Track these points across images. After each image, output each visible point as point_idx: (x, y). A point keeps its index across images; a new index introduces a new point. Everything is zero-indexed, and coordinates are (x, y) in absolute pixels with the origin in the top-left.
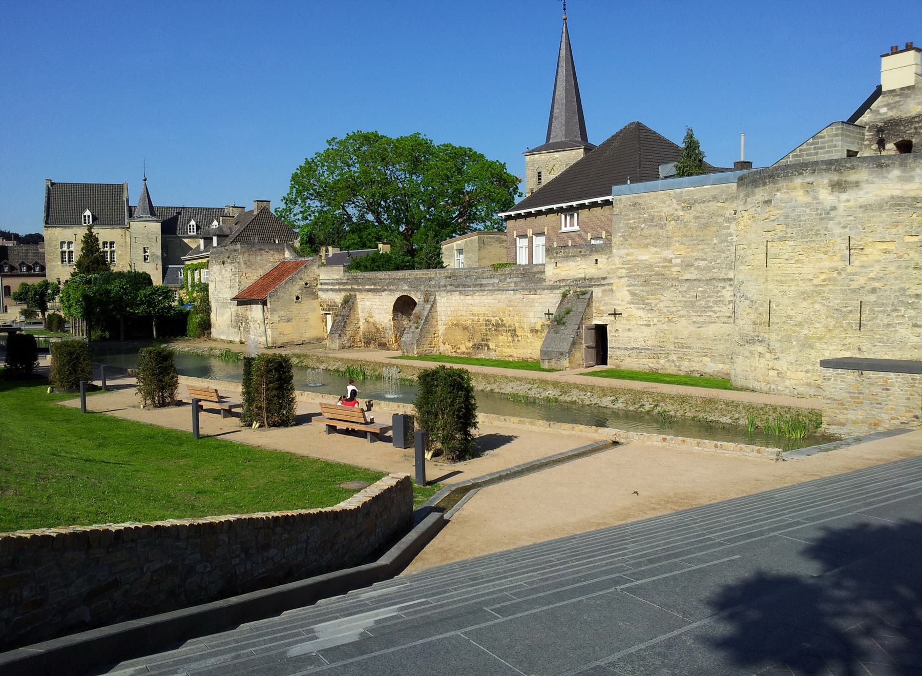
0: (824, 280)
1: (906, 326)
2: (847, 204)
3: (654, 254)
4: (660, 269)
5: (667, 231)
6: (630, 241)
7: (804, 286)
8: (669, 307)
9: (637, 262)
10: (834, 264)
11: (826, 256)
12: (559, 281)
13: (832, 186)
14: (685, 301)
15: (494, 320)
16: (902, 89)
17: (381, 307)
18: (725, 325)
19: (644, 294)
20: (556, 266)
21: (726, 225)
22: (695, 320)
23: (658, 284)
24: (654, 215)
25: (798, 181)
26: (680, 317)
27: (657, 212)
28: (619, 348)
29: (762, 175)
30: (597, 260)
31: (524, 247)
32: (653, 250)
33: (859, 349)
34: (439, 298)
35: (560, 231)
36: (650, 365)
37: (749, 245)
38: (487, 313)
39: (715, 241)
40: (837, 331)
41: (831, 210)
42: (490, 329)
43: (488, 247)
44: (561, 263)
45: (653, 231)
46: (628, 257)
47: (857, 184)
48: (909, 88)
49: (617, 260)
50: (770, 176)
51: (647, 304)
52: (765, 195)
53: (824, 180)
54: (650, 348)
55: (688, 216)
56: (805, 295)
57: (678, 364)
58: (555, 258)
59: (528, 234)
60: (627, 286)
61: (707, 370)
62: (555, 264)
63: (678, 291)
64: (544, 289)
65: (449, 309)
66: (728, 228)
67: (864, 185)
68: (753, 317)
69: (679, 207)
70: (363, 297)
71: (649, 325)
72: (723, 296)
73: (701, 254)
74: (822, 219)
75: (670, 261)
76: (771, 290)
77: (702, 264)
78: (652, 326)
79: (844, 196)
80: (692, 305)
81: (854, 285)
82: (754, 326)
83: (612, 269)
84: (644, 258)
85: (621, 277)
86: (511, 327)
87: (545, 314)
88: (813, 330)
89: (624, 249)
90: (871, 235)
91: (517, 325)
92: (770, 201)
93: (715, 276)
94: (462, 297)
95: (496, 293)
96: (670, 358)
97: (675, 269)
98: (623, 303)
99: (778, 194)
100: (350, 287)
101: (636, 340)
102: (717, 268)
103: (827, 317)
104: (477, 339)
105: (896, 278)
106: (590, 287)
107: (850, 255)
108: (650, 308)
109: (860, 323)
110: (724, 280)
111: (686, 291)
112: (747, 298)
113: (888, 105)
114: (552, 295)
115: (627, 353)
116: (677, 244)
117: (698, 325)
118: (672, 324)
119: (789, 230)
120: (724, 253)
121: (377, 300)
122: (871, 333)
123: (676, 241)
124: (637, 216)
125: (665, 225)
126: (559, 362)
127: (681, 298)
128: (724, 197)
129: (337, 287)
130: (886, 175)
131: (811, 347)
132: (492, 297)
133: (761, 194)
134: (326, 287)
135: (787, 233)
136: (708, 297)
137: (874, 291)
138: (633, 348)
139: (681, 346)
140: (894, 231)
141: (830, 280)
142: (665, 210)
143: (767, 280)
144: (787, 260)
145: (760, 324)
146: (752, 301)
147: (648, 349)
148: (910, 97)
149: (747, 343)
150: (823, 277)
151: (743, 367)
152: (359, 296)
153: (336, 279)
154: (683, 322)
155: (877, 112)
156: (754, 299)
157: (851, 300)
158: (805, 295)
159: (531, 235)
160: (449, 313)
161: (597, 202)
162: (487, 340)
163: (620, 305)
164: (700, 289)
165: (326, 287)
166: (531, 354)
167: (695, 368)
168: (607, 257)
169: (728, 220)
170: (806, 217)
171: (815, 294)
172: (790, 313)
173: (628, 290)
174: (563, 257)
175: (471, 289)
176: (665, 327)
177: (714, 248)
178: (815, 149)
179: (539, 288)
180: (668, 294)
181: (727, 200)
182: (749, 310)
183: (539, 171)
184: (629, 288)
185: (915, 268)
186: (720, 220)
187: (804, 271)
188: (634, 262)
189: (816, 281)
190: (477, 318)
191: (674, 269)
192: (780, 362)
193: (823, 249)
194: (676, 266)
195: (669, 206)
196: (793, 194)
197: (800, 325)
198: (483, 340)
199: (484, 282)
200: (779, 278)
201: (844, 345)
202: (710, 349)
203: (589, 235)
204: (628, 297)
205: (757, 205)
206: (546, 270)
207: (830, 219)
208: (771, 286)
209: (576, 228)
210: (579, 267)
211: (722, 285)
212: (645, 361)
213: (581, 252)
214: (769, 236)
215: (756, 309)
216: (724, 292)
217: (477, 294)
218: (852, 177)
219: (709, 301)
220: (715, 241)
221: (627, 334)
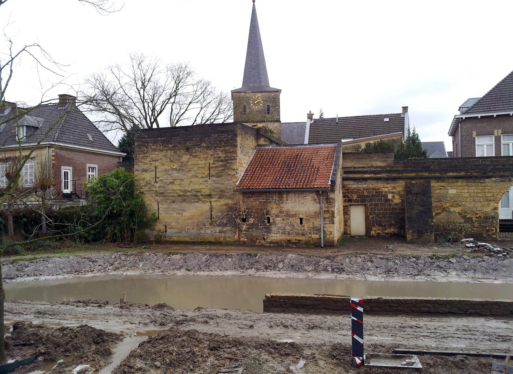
17: (480, 195)
70: (443, 184)
100: (413, 175)
121: (474, 188)
129: (384, 175)
134: (359, 176)
152: (433, 184)
153: (380, 167)
165: (359, 176)
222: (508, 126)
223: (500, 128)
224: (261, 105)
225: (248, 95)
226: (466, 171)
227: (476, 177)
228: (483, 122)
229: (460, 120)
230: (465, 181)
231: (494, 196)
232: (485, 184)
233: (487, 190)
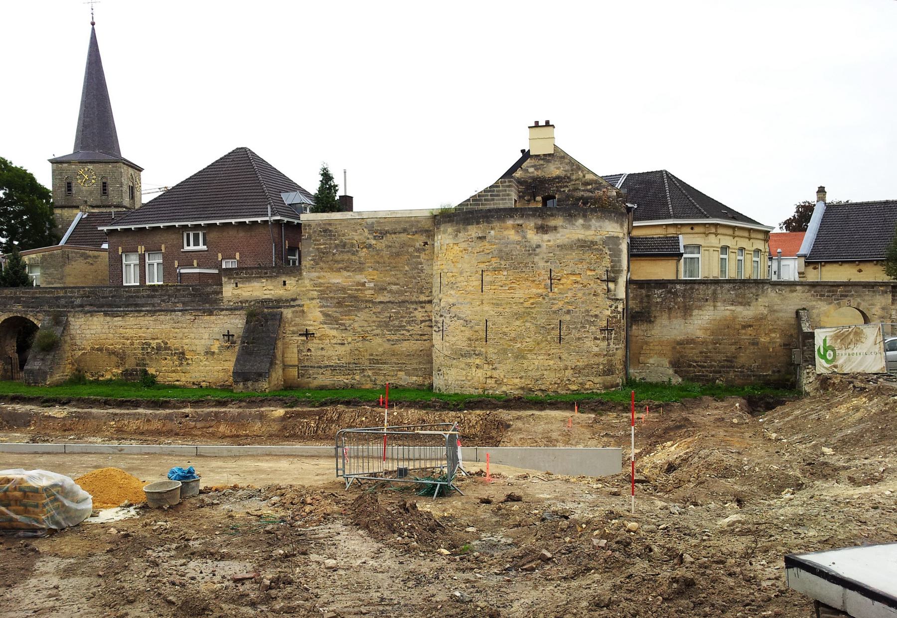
0: (532, 304)
1: (590, 339)
2: (548, 243)
3: (346, 278)
4: (353, 292)
5: (360, 257)
6: (322, 264)
7: (515, 308)
8: (363, 327)
9: (329, 285)
10: (540, 291)
11: (533, 285)
12: (241, 302)
13: (537, 228)
14: (379, 321)
15: (154, 343)
16: (544, 155)
19: (338, 315)
20: (237, 286)
21: (416, 254)
22: (389, 338)
23: (351, 306)
24: (345, 242)
25: (510, 222)
26: (375, 335)
27: (349, 239)
28: (311, 367)
29: (475, 215)
30: (284, 282)
31: (132, 265)
32: (346, 274)
33: (560, 358)
34: (73, 319)
35: (182, 250)
36: (345, 381)
37: (461, 273)
38: (144, 335)
39: (407, 268)
40: (543, 344)
41: (537, 247)
42: (148, 353)
43: (73, 263)
44: (242, 284)
45: (346, 257)
46: (320, 280)
47: (555, 228)
48: (550, 155)
49: (307, 282)
50: (483, 217)
52: (479, 232)
53: (531, 223)
54: (345, 365)
55: (380, 244)
56: (518, 316)
57: (373, 379)
58: (234, 278)
59: (139, 250)
60: (321, 307)
61: (402, 383)
62: (235, 285)
63: (372, 312)
64: (222, 310)
66: (419, 257)
67: (560, 230)
68: (468, 333)
72: (415, 317)
73: (394, 280)
74: (530, 255)
75: (363, 284)
76: (487, 312)
77: (394, 288)
78: (347, 345)
79: (546, 237)
80: (386, 325)
81: (555, 308)
82: (469, 342)
83: (303, 291)
84: (336, 281)
85: (313, 299)
86: (178, 350)
87: (224, 335)
88: (525, 344)
89: (315, 272)
90: (565, 268)
91: (186, 347)
92: (485, 237)
93: (407, 298)
94: (108, 319)
96: (365, 374)
97: (368, 292)
98: (315, 323)
99: (492, 232)
101: (329, 358)
102: (408, 291)
103: (535, 333)
104: (130, 364)
105: (583, 303)
106: (278, 308)
107: (551, 284)
108: (344, 328)
109: (560, 338)
110: (416, 303)
111: (379, 313)
112: (459, 318)
113: (536, 168)
114: (231, 316)
115: (321, 371)
116: (370, 270)
117: (393, 343)
118: (367, 342)
119: (503, 262)
120: (415, 279)
122: (568, 345)
123: (369, 267)
124: (328, 242)
125: (357, 251)
126: (256, 384)
127: (375, 319)
128: (414, 230)
130: (574, 222)
131: (524, 358)
132: (151, 318)
133: (475, 230)
135: (501, 264)
136: (401, 317)
137: (568, 312)
138: (327, 366)
139: (375, 361)
140: (580, 266)
141: (537, 303)
142: (356, 238)
143: (482, 303)
144: (502, 286)
145: (477, 340)
146: (467, 321)
147: (343, 367)
148: (551, 162)
149: (462, 356)
150: (532, 301)
151: (458, 377)
154: (379, 340)
155: (526, 171)
156: (468, 319)
157: (553, 319)
158: (518, 316)
159: (143, 252)
160: (88, 336)
161: (245, 222)
162: (144, 365)
164: (394, 310)
166: (205, 377)
167: (390, 382)
168: (297, 279)
169: (418, 250)
170: (517, 253)
171: (525, 314)
172: (505, 330)
173: (321, 312)
174: (244, 277)
175: (122, 309)
176: (360, 345)
177: (406, 274)
178: (491, 195)
179: (216, 309)
180: (362, 315)
181: (416, 232)
182: (463, 329)
183: (68, 181)
184: (321, 309)
185: (594, 295)
186: (411, 250)
187: (516, 296)
189: (526, 305)
190: (129, 341)
191: (367, 292)
192: (498, 371)
193: (531, 279)
194: (369, 289)
195: (361, 234)
196: (506, 233)
197: (514, 340)
198: (137, 366)
199: (139, 301)
200: (494, 301)
201: (549, 355)
202: (404, 363)
203: (220, 257)
204: (321, 318)
205: (470, 240)
206: (224, 289)
207: (536, 255)
208: (486, 308)
209: (202, 247)
210: (265, 288)
211: (414, 306)
212: (341, 378)
213: (266, 273)
214: (483, 266)
215: (471, 327)
216: (416, 313)
217: (131, 316)
218: (552, 222)
219: (402, 321)
220: (407, 268)
221: (320, 353)
223: (143, 245)
224: (93, 181)
225: (73, 166)
228: (128, 237)
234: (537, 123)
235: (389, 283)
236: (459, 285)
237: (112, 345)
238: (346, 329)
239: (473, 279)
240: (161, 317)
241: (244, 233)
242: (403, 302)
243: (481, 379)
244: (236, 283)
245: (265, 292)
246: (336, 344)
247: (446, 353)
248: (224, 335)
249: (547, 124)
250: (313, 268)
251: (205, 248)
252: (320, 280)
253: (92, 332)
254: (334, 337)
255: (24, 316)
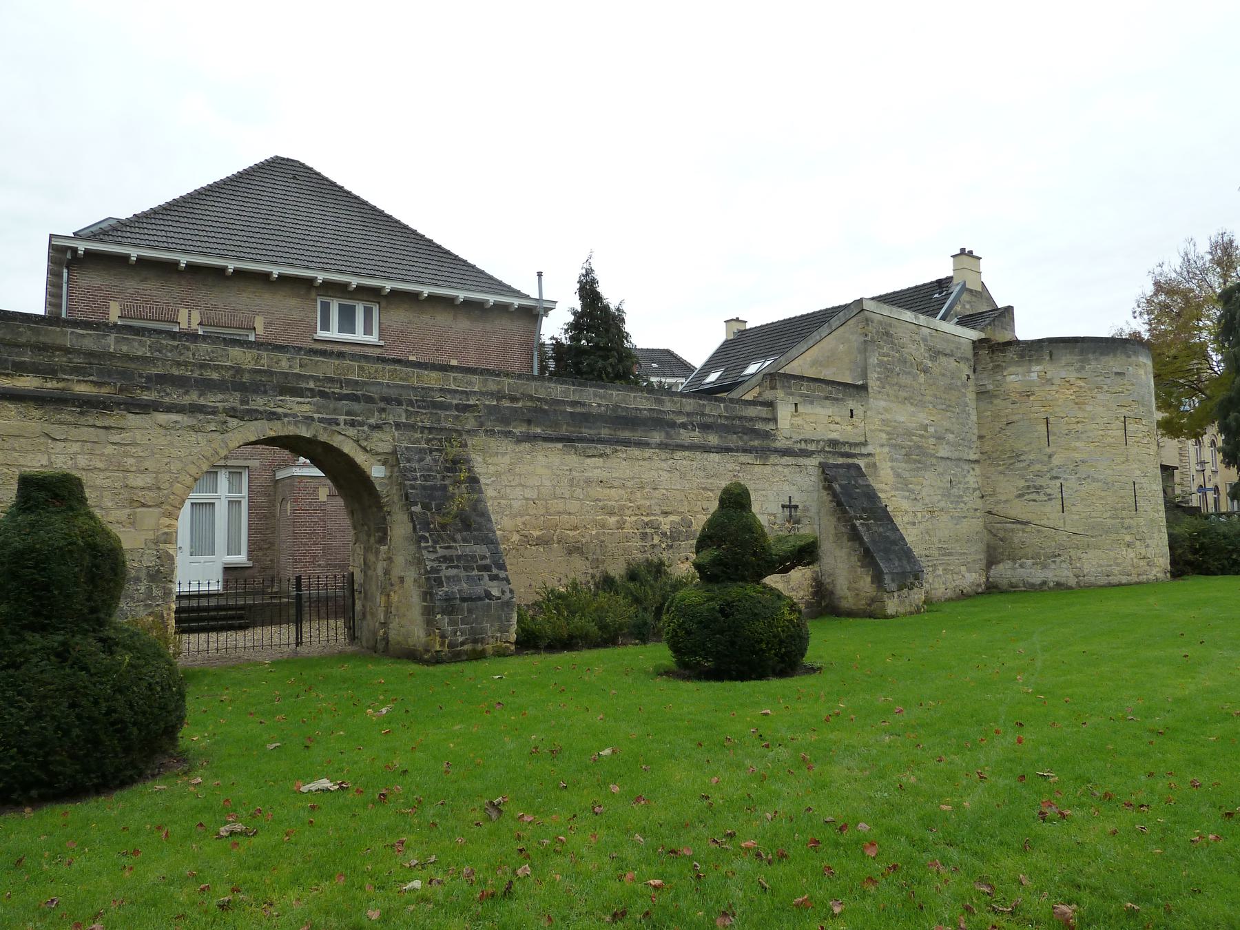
5: (920, 384)
12: (806, 441)
15: (666, 524)
18: (974, 520)
19: (906, 475)
20: (796, 411)
30: (851, 411)
42: (653, 546)
51: (912, 491)
58: (792, 394)
60: (892, 460)
63: (936, 473)
65: (518, 492)
69: (926, 355)
71: (914, 524)
75: (925, 428)
77: (950, 437)
84: (902, 419)
87: (783, 506)
94: (573, 460)
95: (678, 454)
108: (913, 496)
112: (1095, 480)
121: (76, 447)
132: (664, 465)
143: (1127, 460)
146: (1107, 484)
163: (883, 491)
173: (892, 468)
180: (929, 477)
182: (1103, 494)
188: (893, 424)
202: (965, 553)
209: (359, 336)
222: (221, 305)
223: (196, 307)
226: (49, 372)
227: (87, 404)
228: (145, 280)
229: (69, 256)
230: (36, 413)
231: (159, 488)
232: (126, 437)
233: (131, 461)
234: (963, 250)
235: (946, 430)
236: (1091, 434)
237: (576, 528)
238: (916, 499)
239: (1114, 426)
240: (684, 462)
241: (469, 323)
242: (959, 459)
243: (1135, 560)
244: (796, 404)
245: (832, 426)
246: (907, 523)
247: (1074, 530)
248: (783, 506)
249: (971, 252)
250: (880, 392)
251: (373, 339)
252: (888, 416)
253: (530, 493)
254: (907, 512)
255: (323, 437)
